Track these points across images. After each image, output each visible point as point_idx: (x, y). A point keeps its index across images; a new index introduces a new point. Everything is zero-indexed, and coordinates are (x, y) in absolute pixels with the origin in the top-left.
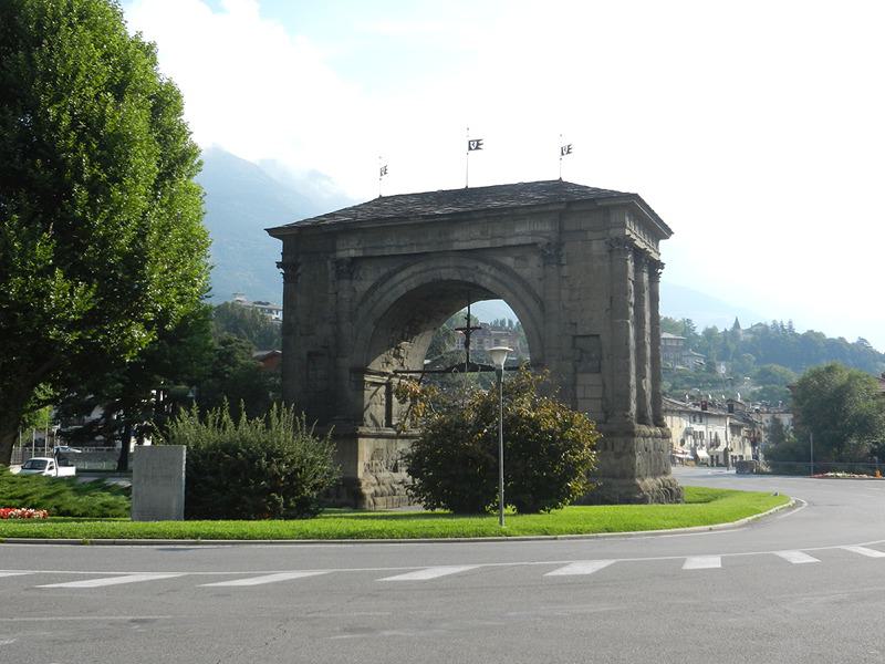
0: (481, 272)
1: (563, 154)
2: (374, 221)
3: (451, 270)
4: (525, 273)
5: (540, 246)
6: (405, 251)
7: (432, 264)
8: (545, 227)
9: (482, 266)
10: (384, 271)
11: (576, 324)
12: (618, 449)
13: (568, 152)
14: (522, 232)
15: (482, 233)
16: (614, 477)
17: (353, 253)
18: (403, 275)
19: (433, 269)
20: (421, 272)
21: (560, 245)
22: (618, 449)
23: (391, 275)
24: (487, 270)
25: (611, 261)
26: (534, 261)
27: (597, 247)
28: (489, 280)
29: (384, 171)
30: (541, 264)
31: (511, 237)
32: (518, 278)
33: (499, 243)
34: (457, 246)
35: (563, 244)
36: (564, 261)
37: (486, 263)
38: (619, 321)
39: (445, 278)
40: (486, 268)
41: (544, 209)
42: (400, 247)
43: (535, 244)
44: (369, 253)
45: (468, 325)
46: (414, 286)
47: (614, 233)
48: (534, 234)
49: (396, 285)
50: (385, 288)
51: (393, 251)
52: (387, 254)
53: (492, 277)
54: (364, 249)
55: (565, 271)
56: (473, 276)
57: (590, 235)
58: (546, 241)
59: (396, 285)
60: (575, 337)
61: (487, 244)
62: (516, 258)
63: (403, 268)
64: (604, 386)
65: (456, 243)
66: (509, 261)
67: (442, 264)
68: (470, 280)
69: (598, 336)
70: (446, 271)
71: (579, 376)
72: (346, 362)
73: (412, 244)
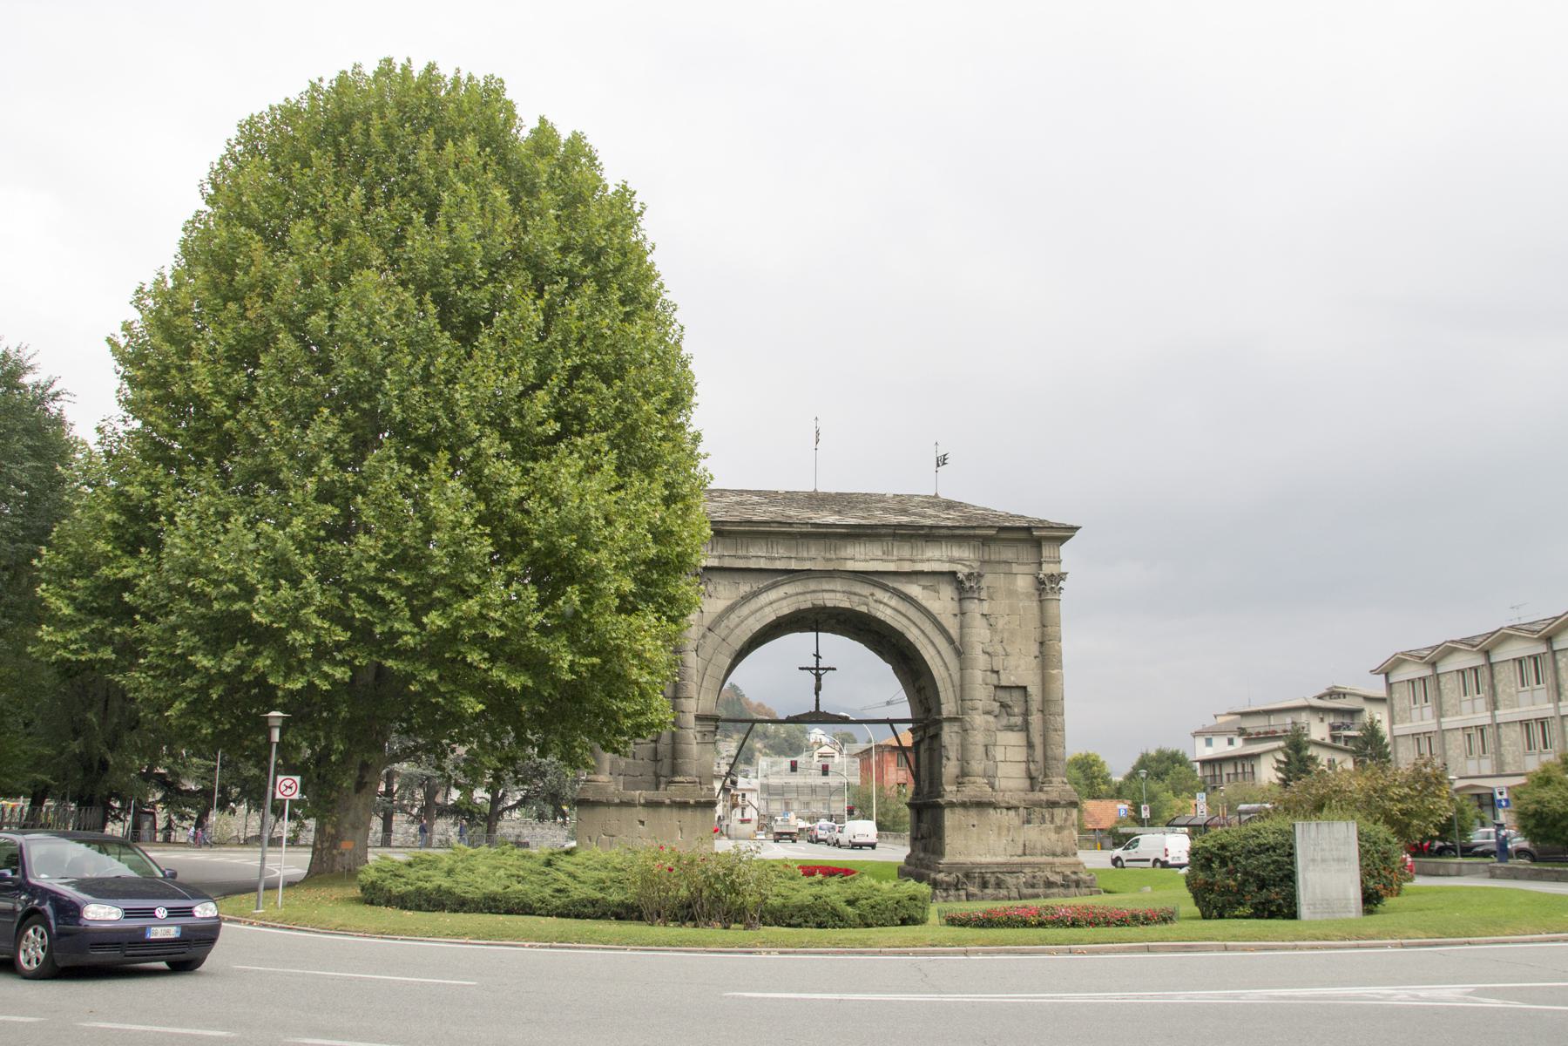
0: (881, 602)
1: (938, 466)
2: (740, 523)
3: (838, 595)
6: (779, 565)
7: (812, 585)
9: (880, 594)
10: (745, 588)
13: (944, 464)
14: (935, 558)
15: (884, 553)
16: (1054, 855)
18: (773, 595)
19: (814, 592)
20: (797, 594)
21: (980, 575)
22: (1058, 822)
23: (755, 594)
24: (885, 600)
25: (1041, 601)
26: (947, 591)
27: (1023, 583)
28: (889, 611)
29: (942, 461)
30: (956, 598)
31: (922, 561)
33: (907, 567)
34: (851, 566)
37: (885, 588)
38: (1055, 672)
39: (829, 604)
41: (971, 532)
43: (954, 573)
44: (727, 563)
45: (817, 664)
46: (786, 611)
47: (1048, 569)
48: (952, 561)
49: (762, 608)
50: (745, 610)
51: (763, 564)
52: (753, 567)
54: (720, 557)
55: (985, 607)
56: (867, 605)
57: (1015, 568)
58: (966, 570)
59: (762, 608)
60: (996, 687)
61: (891, 567)
62: (925, 588)
63: (774, 586)
64: (1030, 745)
66: (914, 590)
67: (826, 587)
68: (864, 609)
69: (1025, 688)
70: (831, 595)
73: (791, 558)
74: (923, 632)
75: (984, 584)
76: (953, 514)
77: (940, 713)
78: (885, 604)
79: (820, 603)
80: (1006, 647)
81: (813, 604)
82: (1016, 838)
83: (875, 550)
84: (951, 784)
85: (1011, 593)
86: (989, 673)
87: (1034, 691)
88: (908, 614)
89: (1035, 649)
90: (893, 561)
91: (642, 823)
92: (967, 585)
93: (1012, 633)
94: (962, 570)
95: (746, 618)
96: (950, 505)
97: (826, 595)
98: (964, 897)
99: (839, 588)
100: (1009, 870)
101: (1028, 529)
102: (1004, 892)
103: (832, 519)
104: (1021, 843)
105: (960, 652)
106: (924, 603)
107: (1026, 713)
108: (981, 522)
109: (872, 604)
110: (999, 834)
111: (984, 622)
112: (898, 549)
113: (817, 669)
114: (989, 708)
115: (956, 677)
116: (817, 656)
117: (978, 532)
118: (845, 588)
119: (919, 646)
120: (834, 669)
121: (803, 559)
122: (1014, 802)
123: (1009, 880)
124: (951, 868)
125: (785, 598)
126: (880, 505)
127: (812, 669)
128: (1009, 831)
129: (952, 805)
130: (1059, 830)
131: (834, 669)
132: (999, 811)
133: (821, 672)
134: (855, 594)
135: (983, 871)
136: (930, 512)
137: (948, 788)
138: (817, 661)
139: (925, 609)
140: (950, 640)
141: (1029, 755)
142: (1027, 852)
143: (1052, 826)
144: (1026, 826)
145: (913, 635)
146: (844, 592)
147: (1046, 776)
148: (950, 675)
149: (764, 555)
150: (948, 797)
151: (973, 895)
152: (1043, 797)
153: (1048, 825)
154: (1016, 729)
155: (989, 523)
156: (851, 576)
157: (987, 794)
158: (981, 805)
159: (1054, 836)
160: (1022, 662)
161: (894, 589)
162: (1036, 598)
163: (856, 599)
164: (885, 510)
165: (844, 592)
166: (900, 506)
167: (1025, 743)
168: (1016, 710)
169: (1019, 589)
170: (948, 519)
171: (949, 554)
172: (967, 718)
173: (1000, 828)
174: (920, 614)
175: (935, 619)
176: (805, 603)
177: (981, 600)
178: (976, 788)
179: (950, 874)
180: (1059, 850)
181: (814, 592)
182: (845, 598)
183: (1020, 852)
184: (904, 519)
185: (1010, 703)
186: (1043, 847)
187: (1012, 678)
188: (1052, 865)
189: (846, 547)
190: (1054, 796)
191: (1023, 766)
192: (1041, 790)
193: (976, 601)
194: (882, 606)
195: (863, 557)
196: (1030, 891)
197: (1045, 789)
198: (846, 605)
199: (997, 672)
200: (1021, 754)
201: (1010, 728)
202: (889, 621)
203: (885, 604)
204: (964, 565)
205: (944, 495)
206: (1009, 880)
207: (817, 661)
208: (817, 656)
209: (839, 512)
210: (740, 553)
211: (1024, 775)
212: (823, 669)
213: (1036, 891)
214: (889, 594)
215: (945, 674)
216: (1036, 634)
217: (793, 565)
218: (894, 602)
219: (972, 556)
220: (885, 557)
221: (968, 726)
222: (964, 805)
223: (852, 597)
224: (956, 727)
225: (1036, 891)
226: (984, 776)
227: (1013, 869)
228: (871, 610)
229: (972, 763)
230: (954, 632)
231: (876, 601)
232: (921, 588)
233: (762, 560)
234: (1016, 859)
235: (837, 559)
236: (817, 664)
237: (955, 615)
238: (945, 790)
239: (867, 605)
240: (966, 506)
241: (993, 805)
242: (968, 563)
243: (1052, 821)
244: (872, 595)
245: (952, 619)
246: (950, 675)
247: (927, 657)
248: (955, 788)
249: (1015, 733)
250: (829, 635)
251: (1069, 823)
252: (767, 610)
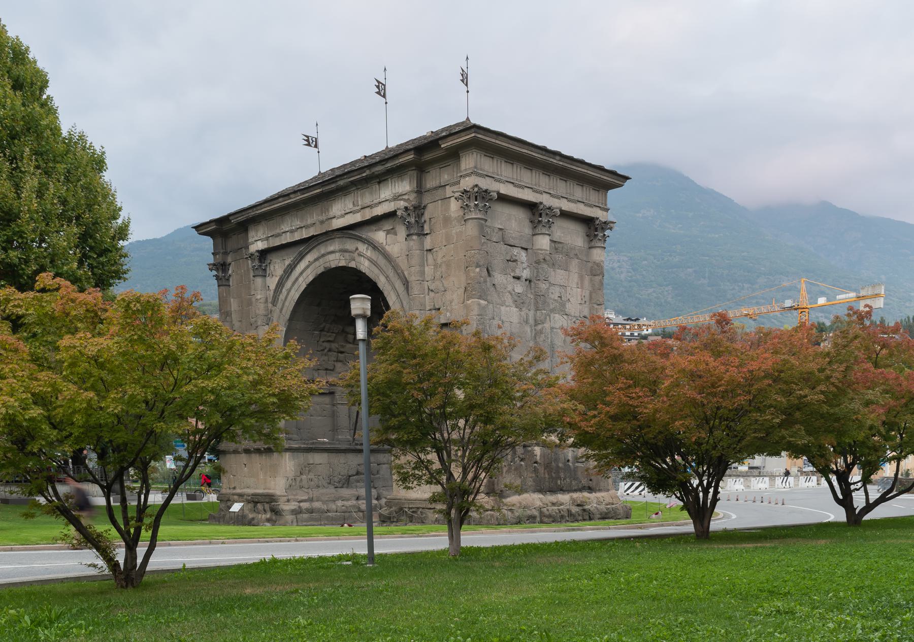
3: (338, 254)
5: (399, 213)
8: (404, 186)
11: (439, 309)
17: (260, 246)
20: (316, 260)
28: (367, 263)
35: (425, 207)
36: (427, 230)
40: (362, 247)
46: (311, 278)
49: (297, 279)
50: (289, 284)
51: (289, 240)
53: (370, 260)
54: (267, 239)
55: (428, 242)
63: (301, 257)
65: (334, 221)
81: (325, 268)
85: (447, 220)
86: (434, 311)
112: (362, 199)
156: (339, 234)
160: (455, 296)
198: (342, 263)
210: (278, 231)
217: (305, 234)
218: (369, 253)
228: (358, 265)
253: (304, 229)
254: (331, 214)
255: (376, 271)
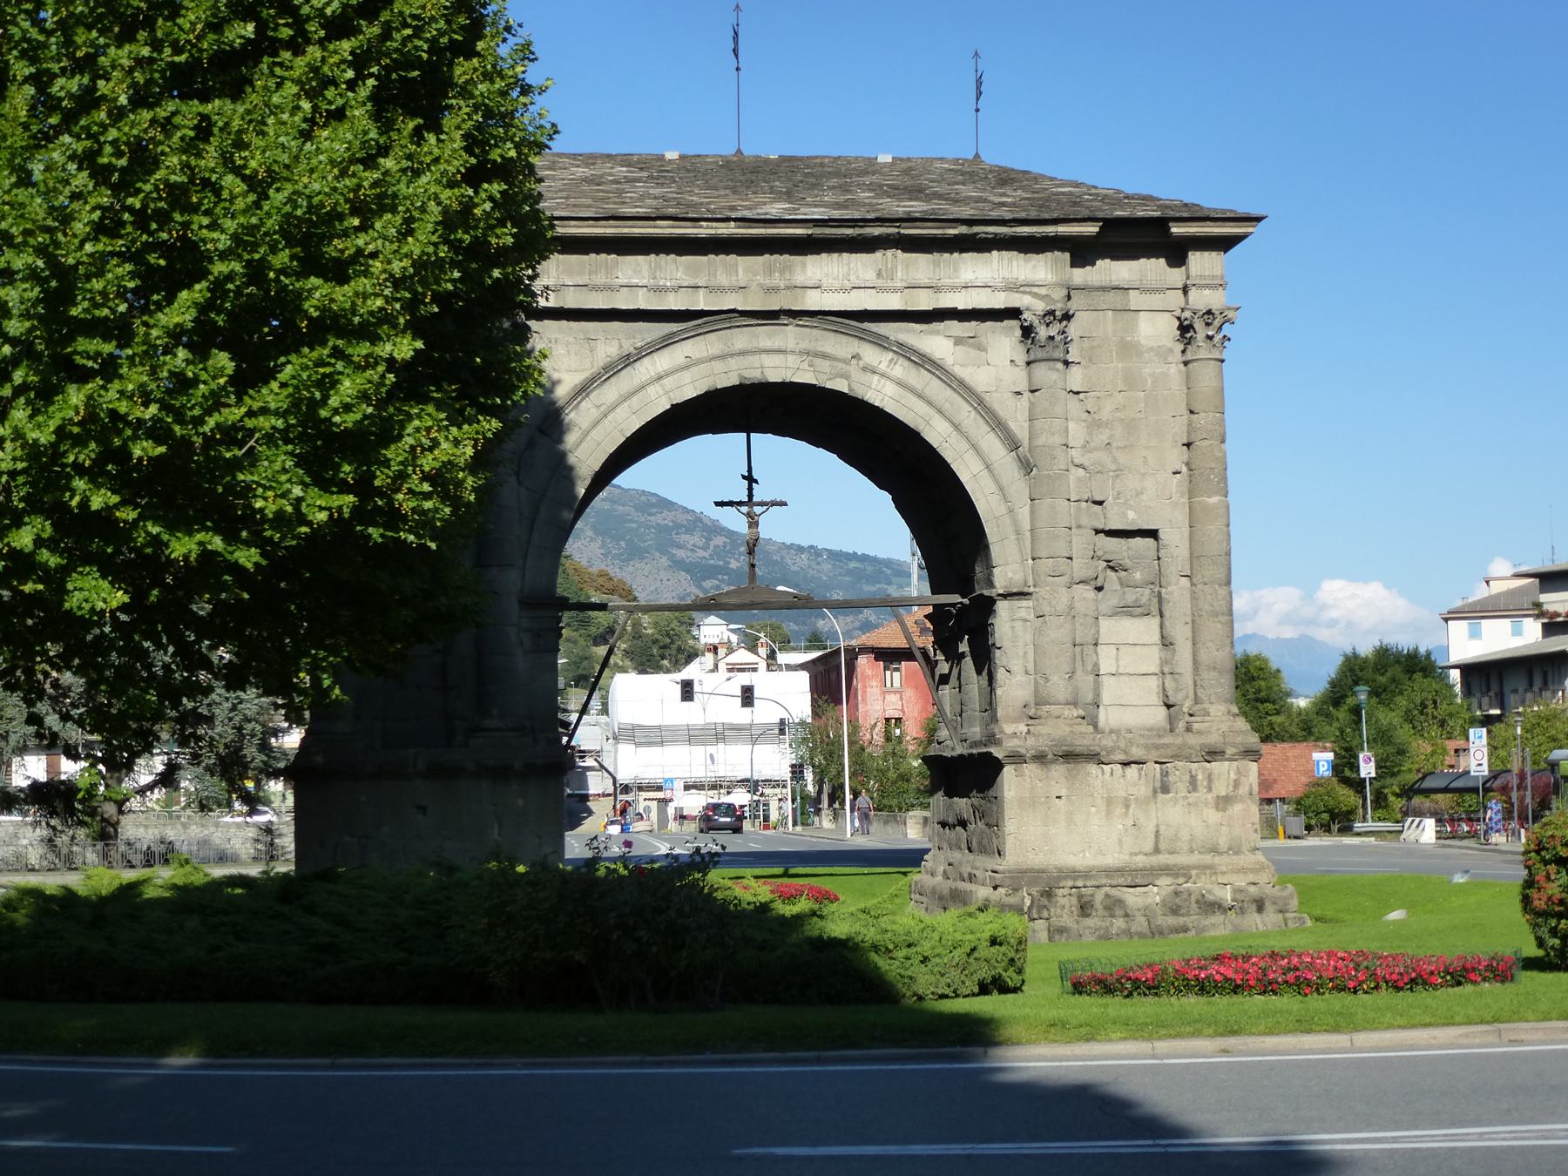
3: (791, 358)
4: (979, 378)
9: (871, 354)
12: (1221, 789)
15: (879, 275)
16: (1215, 850)
19: (743, 353)
23: (628, 361)
24: (883, 367)
25: (1186, 363)
28: (890, 389)
30: (1021, 358)
32: (962, 388)
33: (924, 302)
34: (813, 301)
37: (881, 343)
39: (774, 377)
41: (1050, 230)
42: (659, 290)
43: (1013, 313)
45: (750, 495)
46: (690, 393)
49: (643, 387)
51: (643, 302)
53: (899, 383)
55: (1076, 377)
56: (846, 376)
57: (1135, 300)
58: (1041, 307)
59: (643, 387)
60: (1097, 532)
61: (894, 303)
62: (959, 341)
63: (666, 342)
64: (1166, 643)
67: (767, 343)
68: (841, 386)
69: (1153, 534)
71: (1105, 625)
72: (511, 582)
74: (957, 427)
75: (1074, 329)
76: (1012, 195)
77: (991, 585)
78: (883, 375)
79: (754, 375)
80: (1118, 454)
82: (1142, 821)
83: (861, 266)
84: (1016, 720)
85: (1128, 349)
87: (1175, 538)
88: (927, 392)
89: (1177, 457)
90: (895, 290)
91: (422, 809)
92: (1042, 332)
93: (1131, 426)
94: (1033, 306)
95: (613, 408)
96: (1005, 178)
97: (768, 360)
98: (1044, 936)
99: (791, 345)
100: (1129, 882)
101: (1162, 223)
102: (1119, 923)
103: (775, 209)
104: (1151, 828)
105: (1027, 467)
106: (959, 371)
107: (1157, 581)
108: (1071, 212)
109: (856, 374)
110: (1109, 813)
111: (1073, 403)
113: (750, 501)
114: (1091, 573)
115: (1024, 513)
116: (750, 479)
117: (1062, 229)
118: (804, 345)
119: (948, 456)
120: (783, 504)
121: (721, 290)
122: (1137, 753)
123: (1133, 898)
124: (1019, 878)
125: (687, 367)
126: (867, 180)
127: (740, 503)
128: (1127, 807)
129: (1017, 758)
130: (1223, 802)
131: (783, 504)
132: (1107, 768)
133: (758, 510)
134: (825, 356)
135: (1080, 883)
136: (968, 191)
137: (1009, 729)
138: (750, 489)
139: (961, 383)
140: (1013, 445)
141: (1164, 662)
142: (1162, 846)
143: (1210, 796)
144: (1161, 796)
145: (937, 434)
146: (801, 353)
147: (1197, 700)
148: (1011, 511)
149: (644, 282)
150: (1011, 744)
151: (1061, 930)
152: (1192, 740)
153: (1202, 793)
154: (1139, 610)
155: (1085, 213)
157: (1083, 738)
158: (1070, 756)
159: (1213, 816)
161: (900, 345)
162: (1178, 357)
163: (825, 365)
164: (878, 189)
165: (801, 353)
166: (908, 182)
167: (1156, 638)
168: (1138, 576)
169: (1143, 342)
170: (1003, 204)
171: (1007, 275)
172: (1042, 592)
173: (1110, 801)
174: (949, 392)
175: (981, 402)
176: (726, 376)
177: (1066, 363)
178: (1059, 728)
179: (1016, 890)
180: (1223, 843)
181: (743, 353)
182: (805, 365)
183: (1149, 846)
184: (917, 207)
185: (1127, 563)
186: (1192, 838)
187: (1131, 515)
188: (1211, 868)
189: (804, 265)
190: (1213, 739)
191: (1153, 683)
192: (1188, 729)
193: (1060, 366)
194: (876, 377)
195: (837, 284)
196: (1171, 921)
197: (1196, 726)
198: (806, 377)
199: (1100, 503)
200: (1151, 659)
201: (1127, 610)
202: (890, 408)
203: (883, 375)
204: (1036, 295)
205: (994, 157)
206: (1133, 898)
207: (750, 489)
208: (750, 479)
209: (789, 196)
211: (1155, 699)
212: (762, 504)
213: (1181, 920)
214: (891, 355)
215: (1002, 509)
216: (1178, 429)
217: (701, 302)
218: (901, 369)
219: (1050, 276)
220: (880, 283)
221: (1046, 609)
222: (1040, 758)
223: (818, 361)
224: (1023, 608)
225: (1181, 920)
226: (1075, 704)
227: (1138, 878)
229: (1055, 678)
230: (1019, 427)
231: (865, 369)
232: (951, 343)
233: (641, 292)
234: (1141, 861)
235: (788, 288)
236: (750, 495)
237: (1019, 393)
238: (1002, 732)
239: (846, 376)
240: (1036, 178)
241: (1095, 758)
242: (1043, 291)
243: (1210, 789)
244: (856, 357)
245: (1011, 401)
246: (1011, 511)
247: (964, 477)
248: (1023, 728)
249: (1136, 621)
250: (769, 438)
251: (1244, 790)
252: (652, 390)
253: (702, 291)
254: (799, 279)
255: (921, 407)
